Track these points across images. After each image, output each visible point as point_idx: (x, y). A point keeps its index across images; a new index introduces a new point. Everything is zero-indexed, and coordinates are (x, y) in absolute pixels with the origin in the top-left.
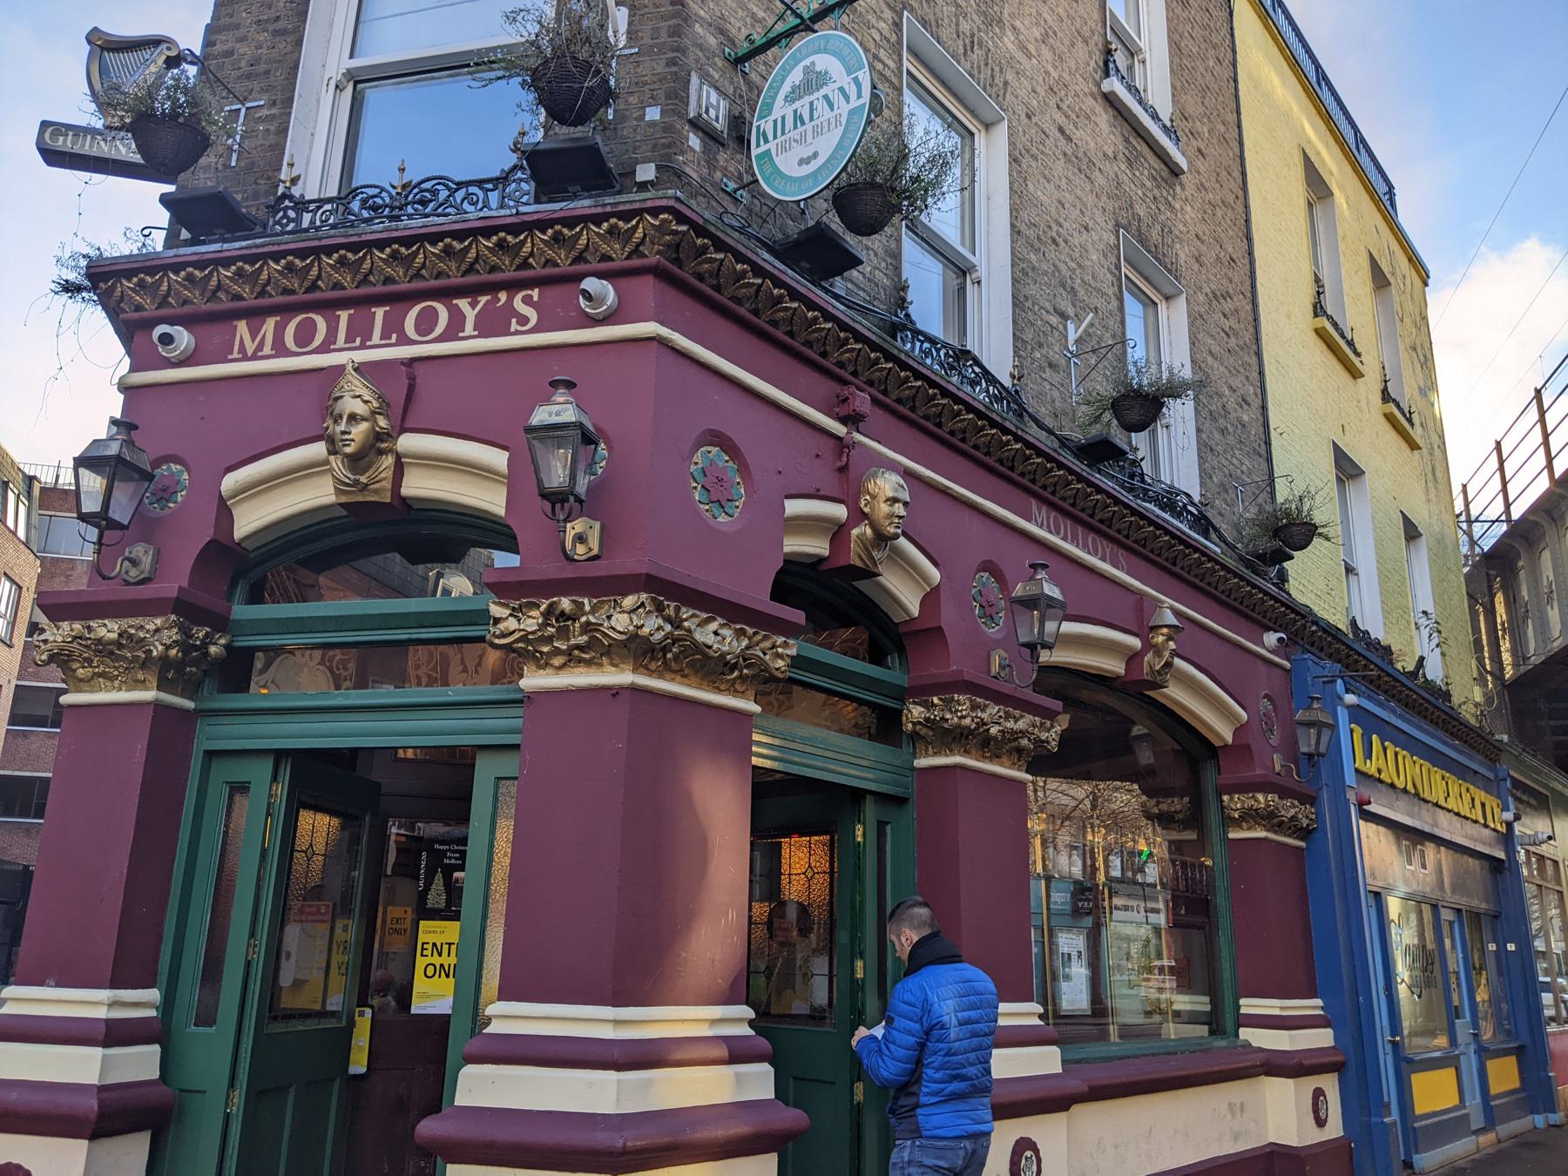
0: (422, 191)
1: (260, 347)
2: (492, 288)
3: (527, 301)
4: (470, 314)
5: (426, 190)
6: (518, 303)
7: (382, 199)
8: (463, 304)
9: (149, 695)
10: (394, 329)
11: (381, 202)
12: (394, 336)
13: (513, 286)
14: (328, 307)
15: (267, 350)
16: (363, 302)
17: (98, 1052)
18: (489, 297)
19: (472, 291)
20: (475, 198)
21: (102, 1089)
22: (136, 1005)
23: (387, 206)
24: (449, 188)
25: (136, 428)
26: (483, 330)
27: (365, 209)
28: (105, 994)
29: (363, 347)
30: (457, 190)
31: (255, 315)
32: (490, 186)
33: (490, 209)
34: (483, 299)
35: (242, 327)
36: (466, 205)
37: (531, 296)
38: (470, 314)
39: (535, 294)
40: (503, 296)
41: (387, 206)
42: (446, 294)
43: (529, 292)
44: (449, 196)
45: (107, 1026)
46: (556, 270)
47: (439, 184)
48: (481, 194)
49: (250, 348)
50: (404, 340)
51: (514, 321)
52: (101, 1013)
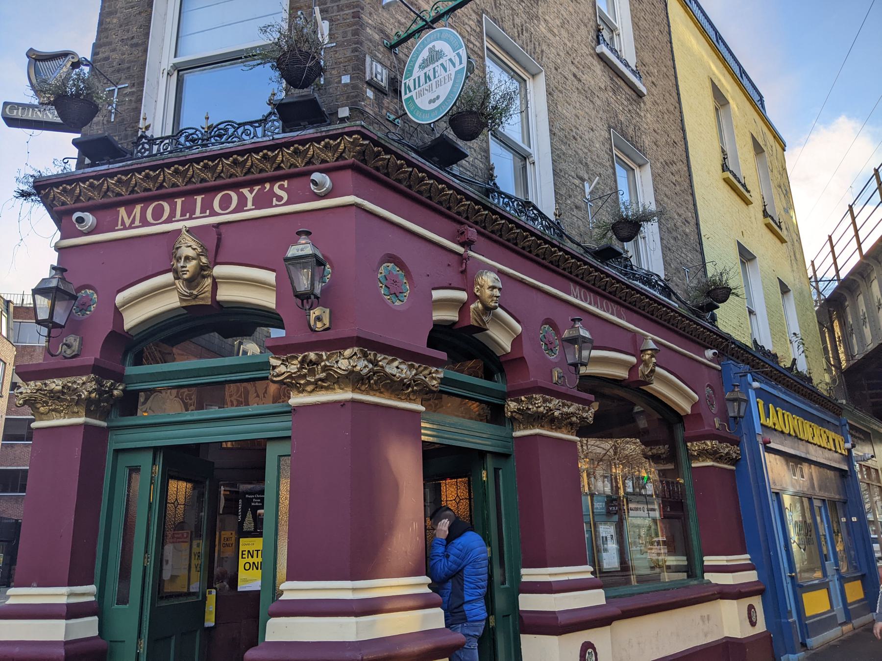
0: (219, 130)
1: (133, 222)
2: (261, 182)
3: (281, 187)
4: (250, 197)
5: (221, 129)
6: (276, 189)
7: (197, 135)
8: (245, 191)
9: (81, 420)
10: (207, 207)
11: (196, 137)
12: (208, 211)
13: (273, 180)
14: (170, 197)
15: (137, 223)
16: (189, 194)
17: (63, 622)
18: (260, 187)
19: (250, 184)
20: (249, 132)
21: (66, 643)
23: (200, 139)
24: (234, 127)
25: (66, 270)
26: (258, 205)
27: (188, 141)
28: (65, 590)
29: (191, 218)
30: (238, 128)
31: (129, 204)
32: (257, 125)
33: (258, 138)
34: (257, 188)
35: (122, 211)
36: (244, 136)
37: (284, 185)
38: (250, 197)
39: (286, 183)
40: (268, 186)
41: (200, 139)
42: (236, 186)
43: (282, 183)
44: (234, 132)
45: (67, 606)
46: (296, 170)
47: (228, 125)
48: (252, 129)
49: (128, 222)
50: (214, 214)
51: (274, 199)
52: (64, 600)
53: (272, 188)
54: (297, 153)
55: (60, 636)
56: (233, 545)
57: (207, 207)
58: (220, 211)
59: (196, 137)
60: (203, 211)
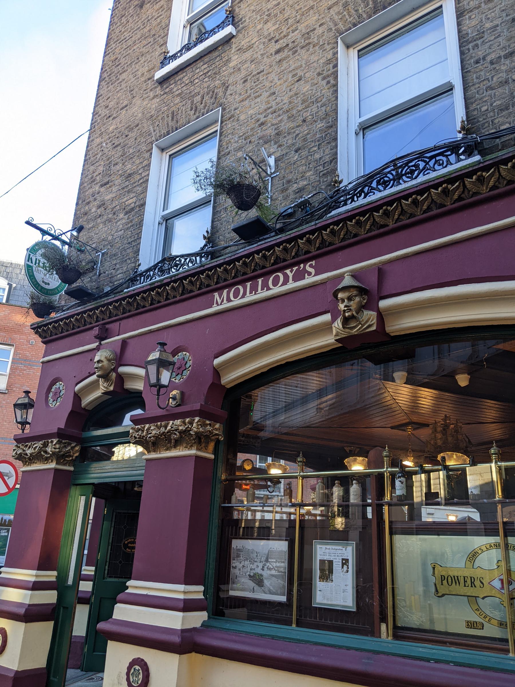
0: (409, 167)
1: (223, 301)
2: (298, 263)
3: (311, 266)
4: (291, 275)
5: (412, 166)
6: (308, 268)
7: (388, 177)
8: (288, 271)
9: (193, 452)
10: (265, 286)
11: (388, 179)
12: (265, 288)
13: (305, 261)
14: (242, 282)
15: (225, 301)
16: (254, 278)
17: (181, 614)
18: (297, 267)
19: (290, 266)
20: (441, 162)
21: (183, 631)
22: (136, 587)
23: (391, 180)
24: (425, 161)
25: (166, 344)
26: (295, 280)
27: (380, 185)
28: (181, 587)
29: (255, 294)
30: (429, 161)
31: (220, 289)
32: (449, 153)
33: (451, 164)
34: (295, 269)
35: (216, 295)
36: (436, 167)
37: (312, 264)
38: (291, 275)
39: (313, 263)
40: (302, 266)
41: (391, 180)
42: (281, 269)
43: (311, 263)
44: (425, 165)
45: (184, 603)
46: (311, 255)
47: (419, 161)
48: (444, 159)
49: (219, 301)
50: (269, 289)
51: (306, 274)
52: (181, 596)
53: (305, 267)
54: (359, 223)
55: (178, 626)
56: (317, 573)
57: (265, 286)
58: (273, 287)
59: (388, 179)
60: (262, 289)
